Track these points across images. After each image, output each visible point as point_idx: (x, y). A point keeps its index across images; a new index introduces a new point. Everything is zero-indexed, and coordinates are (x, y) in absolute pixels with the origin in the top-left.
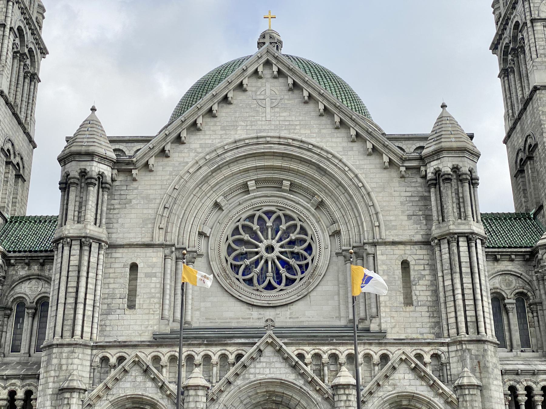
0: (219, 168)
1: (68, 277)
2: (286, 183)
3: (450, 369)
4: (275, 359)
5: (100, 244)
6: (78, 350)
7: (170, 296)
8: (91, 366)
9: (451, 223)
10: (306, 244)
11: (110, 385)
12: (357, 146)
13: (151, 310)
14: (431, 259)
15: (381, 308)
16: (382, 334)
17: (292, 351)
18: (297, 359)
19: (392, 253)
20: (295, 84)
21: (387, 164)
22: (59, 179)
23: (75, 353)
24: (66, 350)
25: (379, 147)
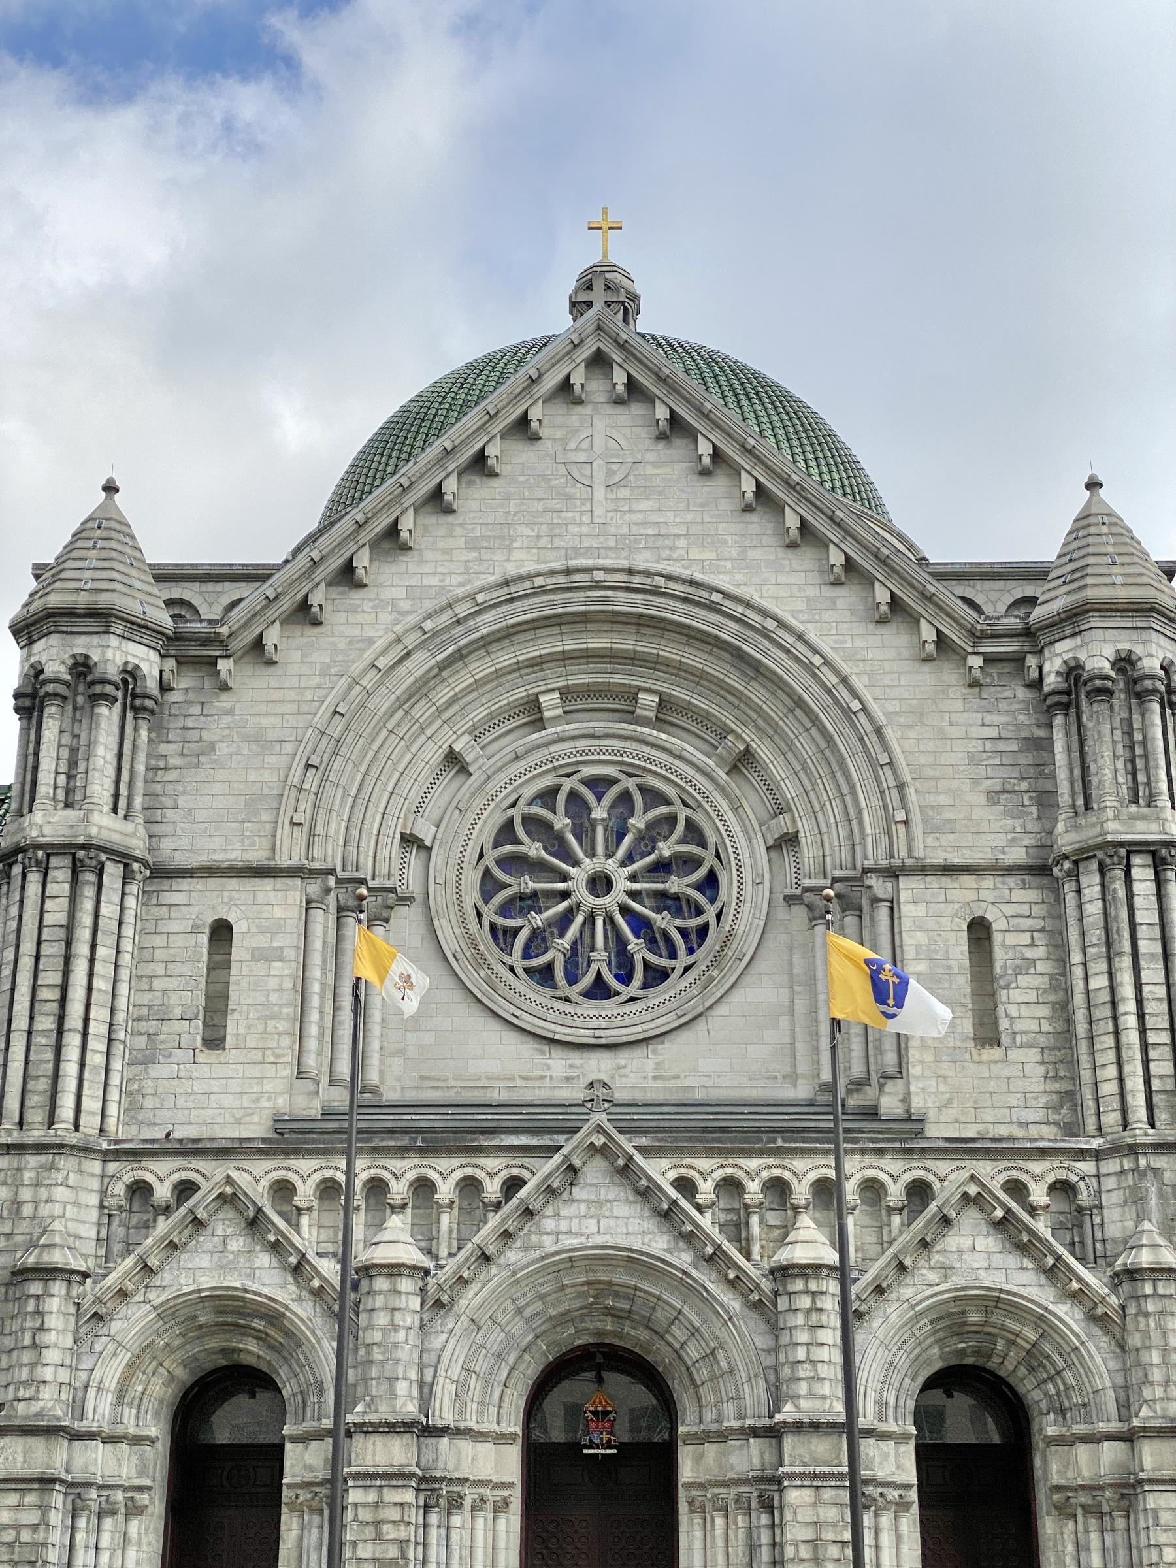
0: (460, 656)
1: (37, 958)
2: (648, 701)
3: (1102, 1225)
4: (612, 1193)
5: (126, 865)
6: (66, 1163)
7: (321, 1012)
8: (102, 1207)
9: (1110, 813)
10: (701, 873)
11: (153, 1262)
12: (847, 596)
13: (269, 1052)
14: (1051, 916)
15: (911, 1052)
16: (913, 1124)
17: (661, 1171)
18: (673, 1194)
19: (942, 899)
20: (674, 419)
21: (930, 648)
22: (13, 682)
23: (58, 1169)
24: (33, 1161)
25: (909, 598)
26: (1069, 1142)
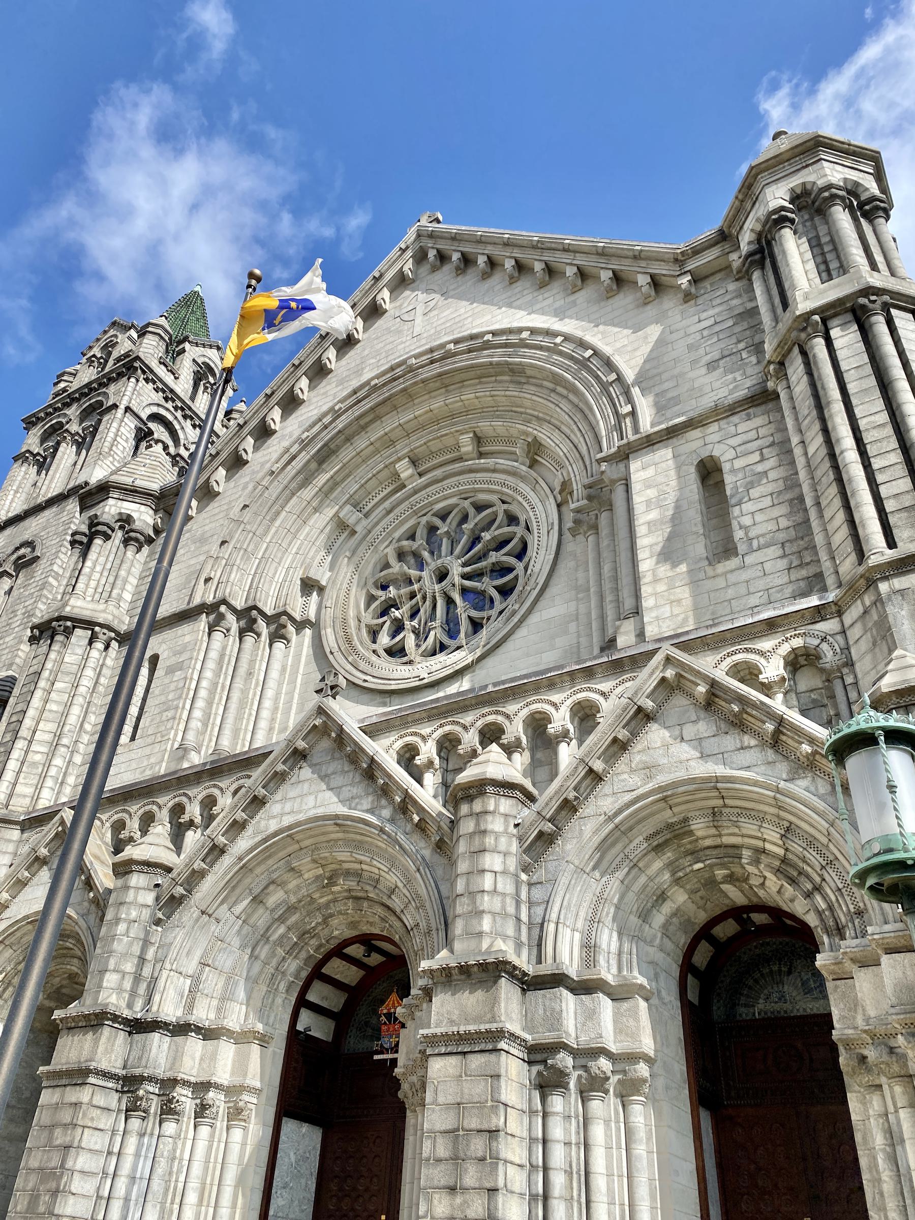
15: (643, 589)
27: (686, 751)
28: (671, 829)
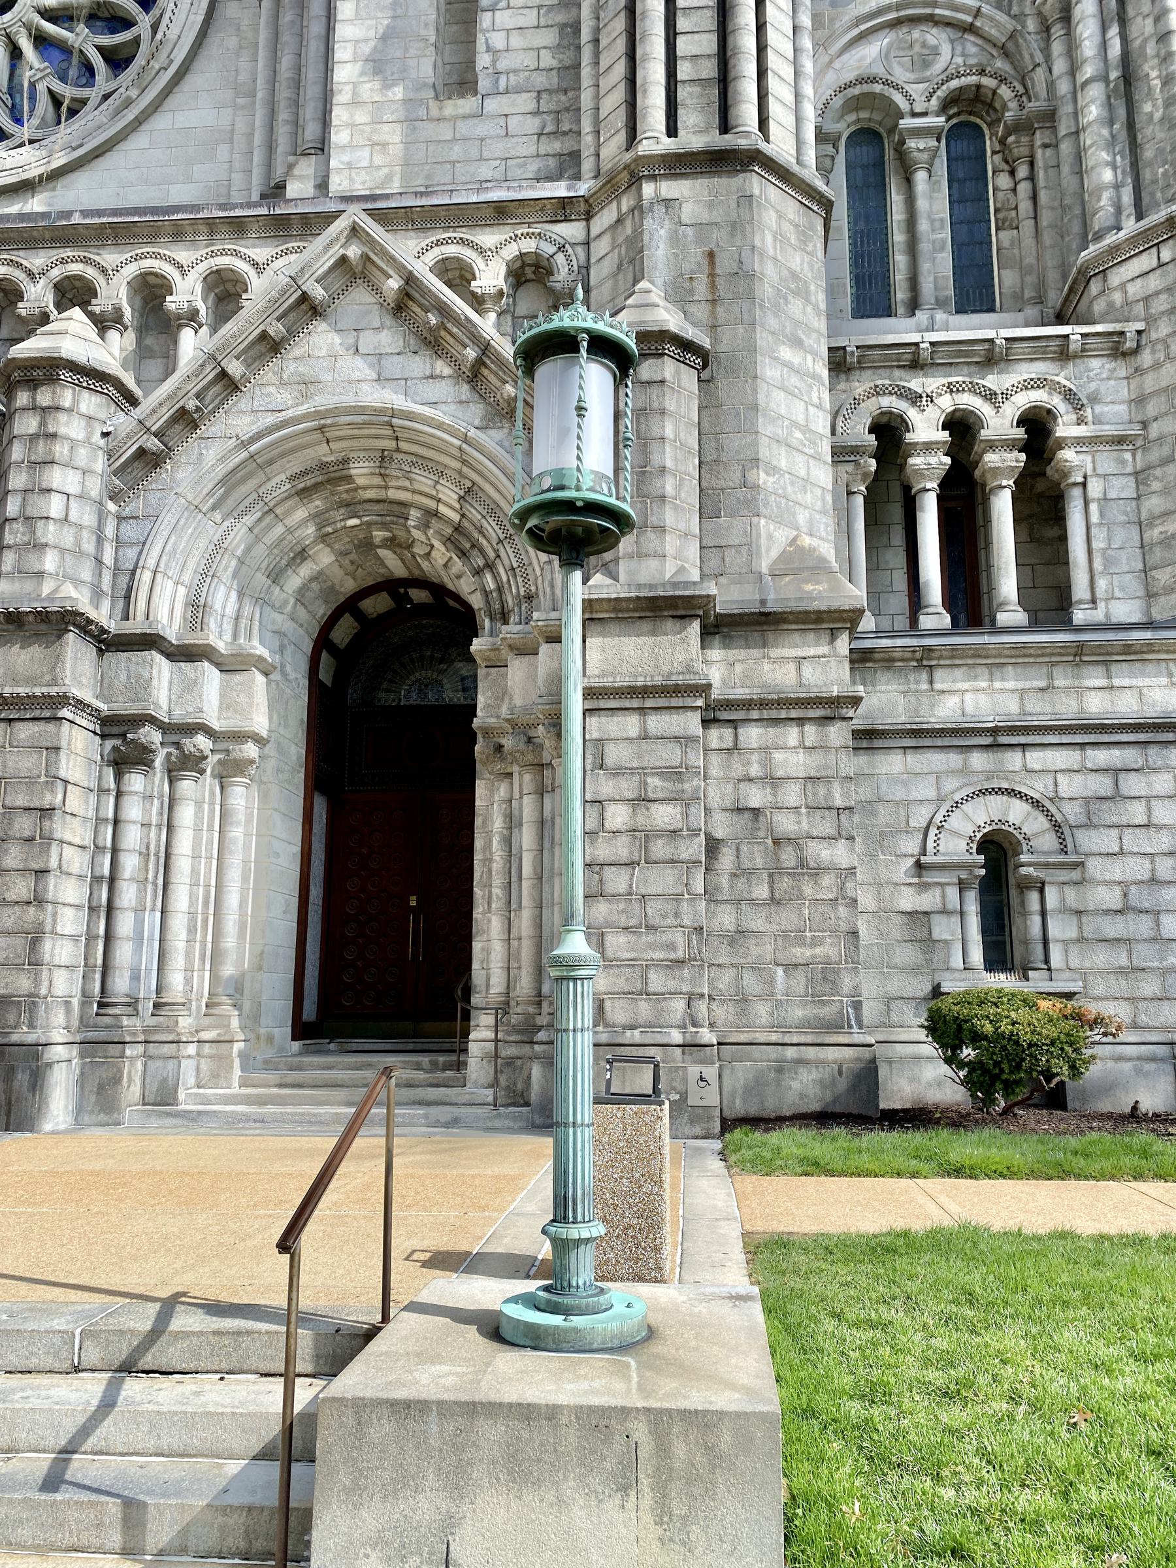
26: (542, 189)
27: (359, 368)
28: (327, 471)
